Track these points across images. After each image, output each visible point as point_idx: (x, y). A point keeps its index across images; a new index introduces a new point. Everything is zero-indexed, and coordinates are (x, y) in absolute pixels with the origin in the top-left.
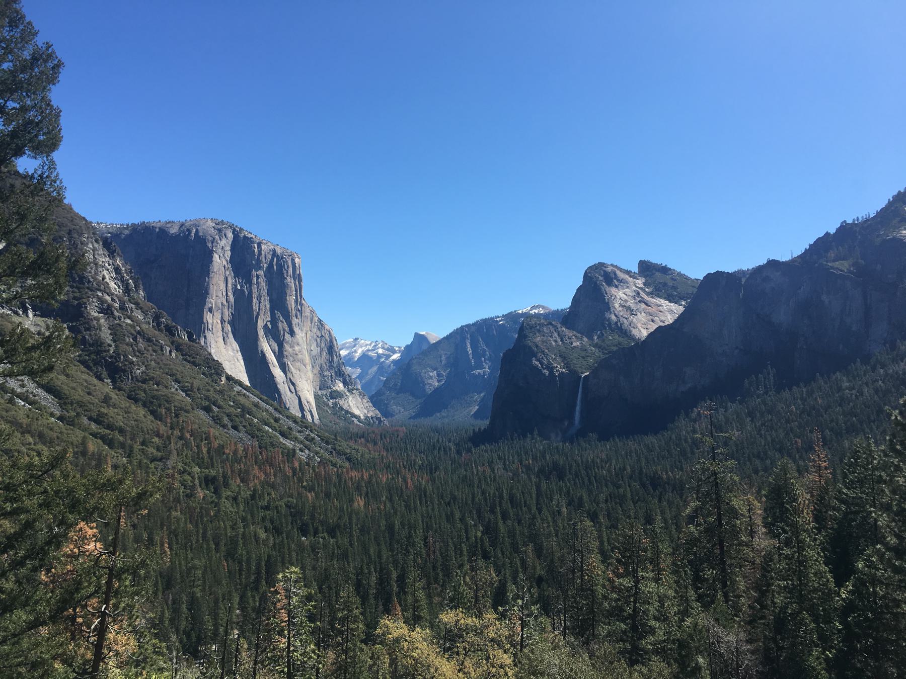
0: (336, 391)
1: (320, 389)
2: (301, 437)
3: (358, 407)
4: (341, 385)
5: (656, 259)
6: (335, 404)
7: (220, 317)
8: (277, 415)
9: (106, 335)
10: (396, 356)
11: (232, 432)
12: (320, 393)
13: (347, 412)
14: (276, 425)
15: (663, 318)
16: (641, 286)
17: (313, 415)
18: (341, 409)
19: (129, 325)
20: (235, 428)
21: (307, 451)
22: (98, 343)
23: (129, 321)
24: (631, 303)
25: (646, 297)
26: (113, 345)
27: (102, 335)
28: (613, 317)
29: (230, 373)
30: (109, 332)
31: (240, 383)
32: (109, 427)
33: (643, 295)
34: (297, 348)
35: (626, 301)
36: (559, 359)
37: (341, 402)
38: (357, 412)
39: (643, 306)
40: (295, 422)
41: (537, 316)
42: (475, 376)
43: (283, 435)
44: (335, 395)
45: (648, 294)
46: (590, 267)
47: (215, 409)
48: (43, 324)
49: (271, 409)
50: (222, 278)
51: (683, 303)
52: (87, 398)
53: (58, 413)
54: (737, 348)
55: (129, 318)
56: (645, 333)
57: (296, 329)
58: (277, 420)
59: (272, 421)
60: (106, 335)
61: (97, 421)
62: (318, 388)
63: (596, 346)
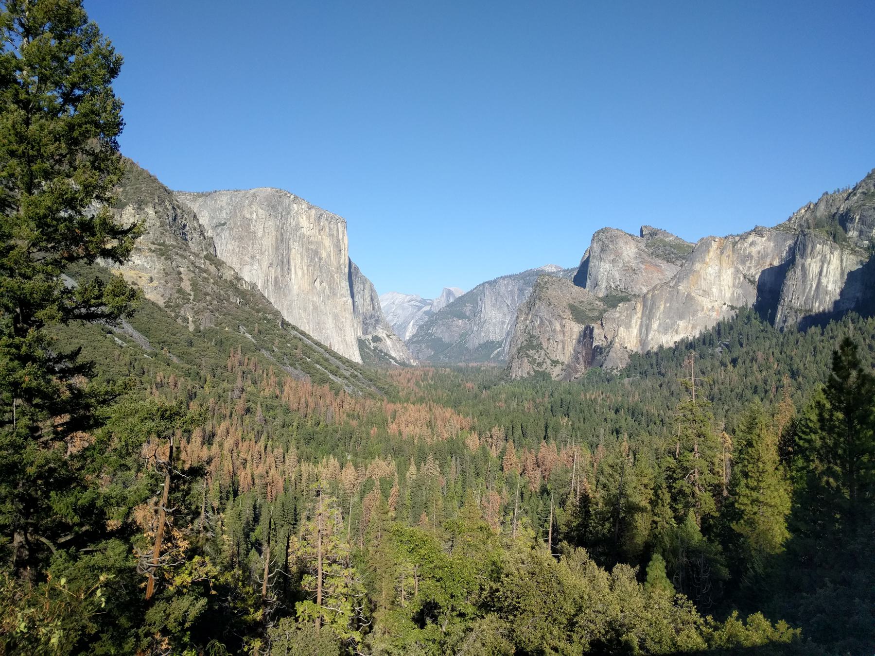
0: (376, 336)
1: (363, 334)
2: (347, 374)
3: (394, 350)
4: (381, 331)
5: (656, 226)
6: (376, 348)
7: (279, 269)
8: (327, 356)
9: (186, 286)
10: (427, 308)
11: (290, 369)
12: (363, 338)
13: (386, 354)
14: (326, 363)
15: (661, 277)
16: (643, 247)
17: (357, 358)
18: (381, 351)
19: (205, 278)
20: (291, 365)
21: (352, 387)
22: (180, 291)
23: (205, 275)
24: (633, 264)
25: (647, 258)
26: (192, 293)
27: (182, 285)
28: (617, 276)
29: (286, 319)
30: (189, 283)
31: (294, 328)
32: (190, 362)
33: (645, 255)
34: (344, 299)
35: (629, 262)
36: (568, 314)
37: (380, 346)
38: (393, 354)
39: (643, 266)
40: (343, 363)
41: (549, 274)
42: (495, 325)
43: (331, 372)
44: (376, 339)
45: (649, 255)
46: (598, 232)
47: (276, 350)
48: (135, 276)
49: (322, 351)
50: (279, 237)
51: (679, 263)
52: (172, 338)
53: (149, 351)
54: (725, 304)
55: (205, 271)
56: (645, 290)
57: (343, 285)
58: (327, 360)
59: (322, 360)
60: (186, 286)
61: (180, 356)
62: (360, 333)
63: (600, 299)
